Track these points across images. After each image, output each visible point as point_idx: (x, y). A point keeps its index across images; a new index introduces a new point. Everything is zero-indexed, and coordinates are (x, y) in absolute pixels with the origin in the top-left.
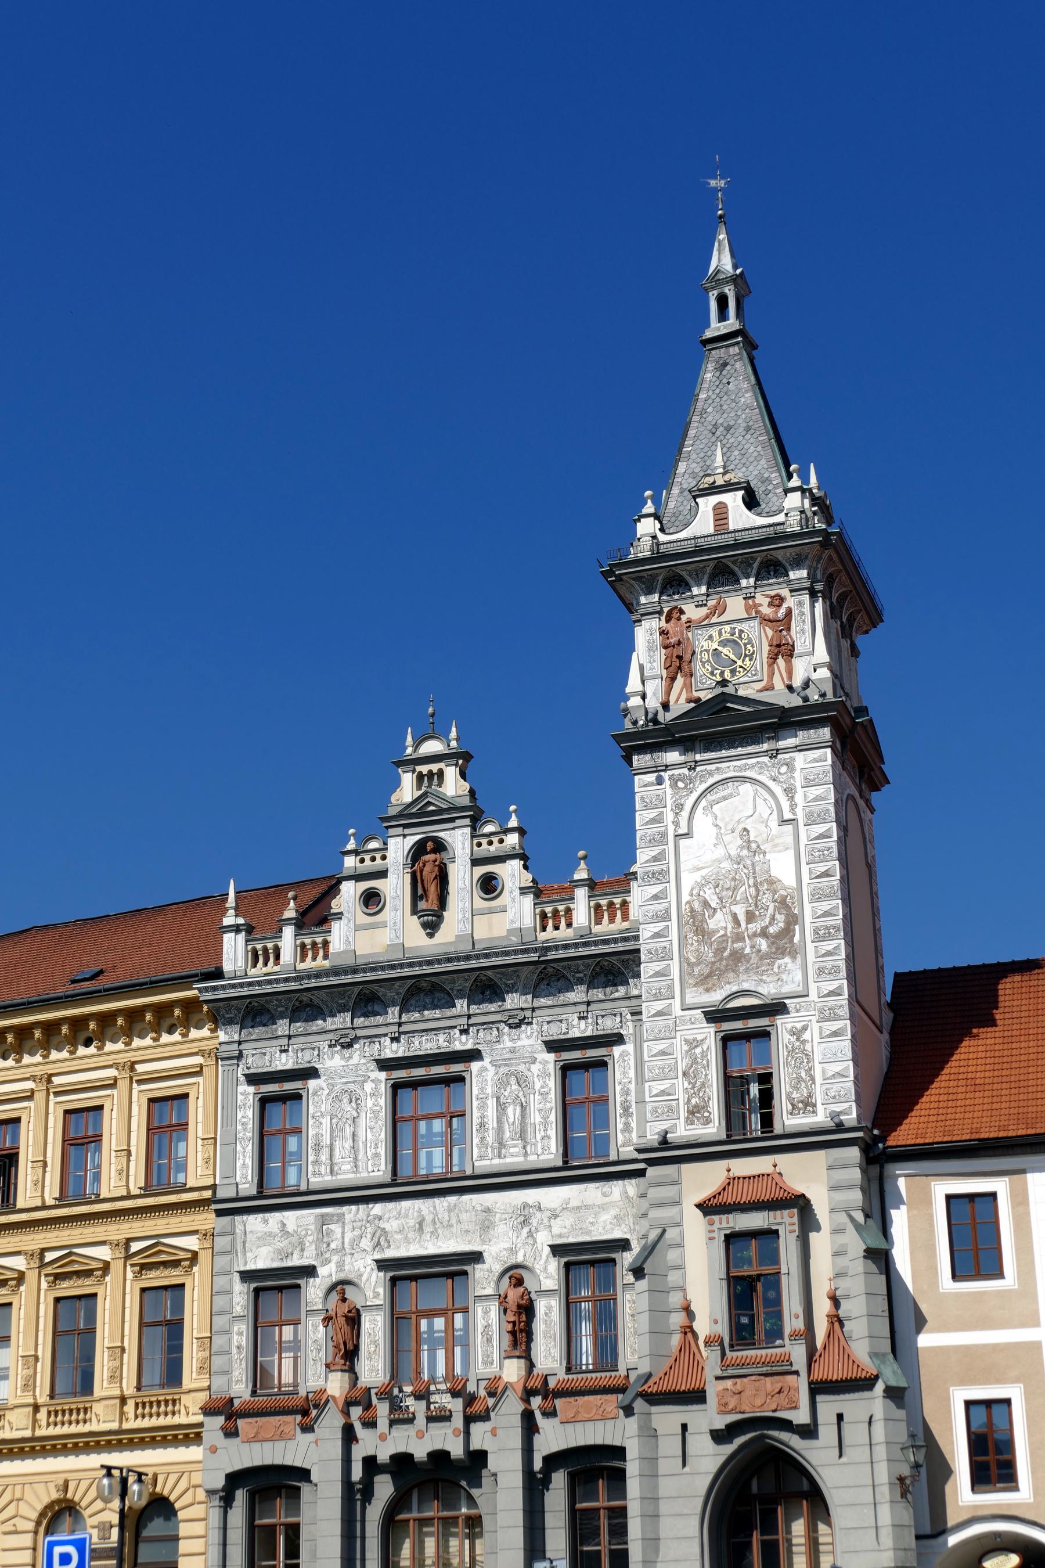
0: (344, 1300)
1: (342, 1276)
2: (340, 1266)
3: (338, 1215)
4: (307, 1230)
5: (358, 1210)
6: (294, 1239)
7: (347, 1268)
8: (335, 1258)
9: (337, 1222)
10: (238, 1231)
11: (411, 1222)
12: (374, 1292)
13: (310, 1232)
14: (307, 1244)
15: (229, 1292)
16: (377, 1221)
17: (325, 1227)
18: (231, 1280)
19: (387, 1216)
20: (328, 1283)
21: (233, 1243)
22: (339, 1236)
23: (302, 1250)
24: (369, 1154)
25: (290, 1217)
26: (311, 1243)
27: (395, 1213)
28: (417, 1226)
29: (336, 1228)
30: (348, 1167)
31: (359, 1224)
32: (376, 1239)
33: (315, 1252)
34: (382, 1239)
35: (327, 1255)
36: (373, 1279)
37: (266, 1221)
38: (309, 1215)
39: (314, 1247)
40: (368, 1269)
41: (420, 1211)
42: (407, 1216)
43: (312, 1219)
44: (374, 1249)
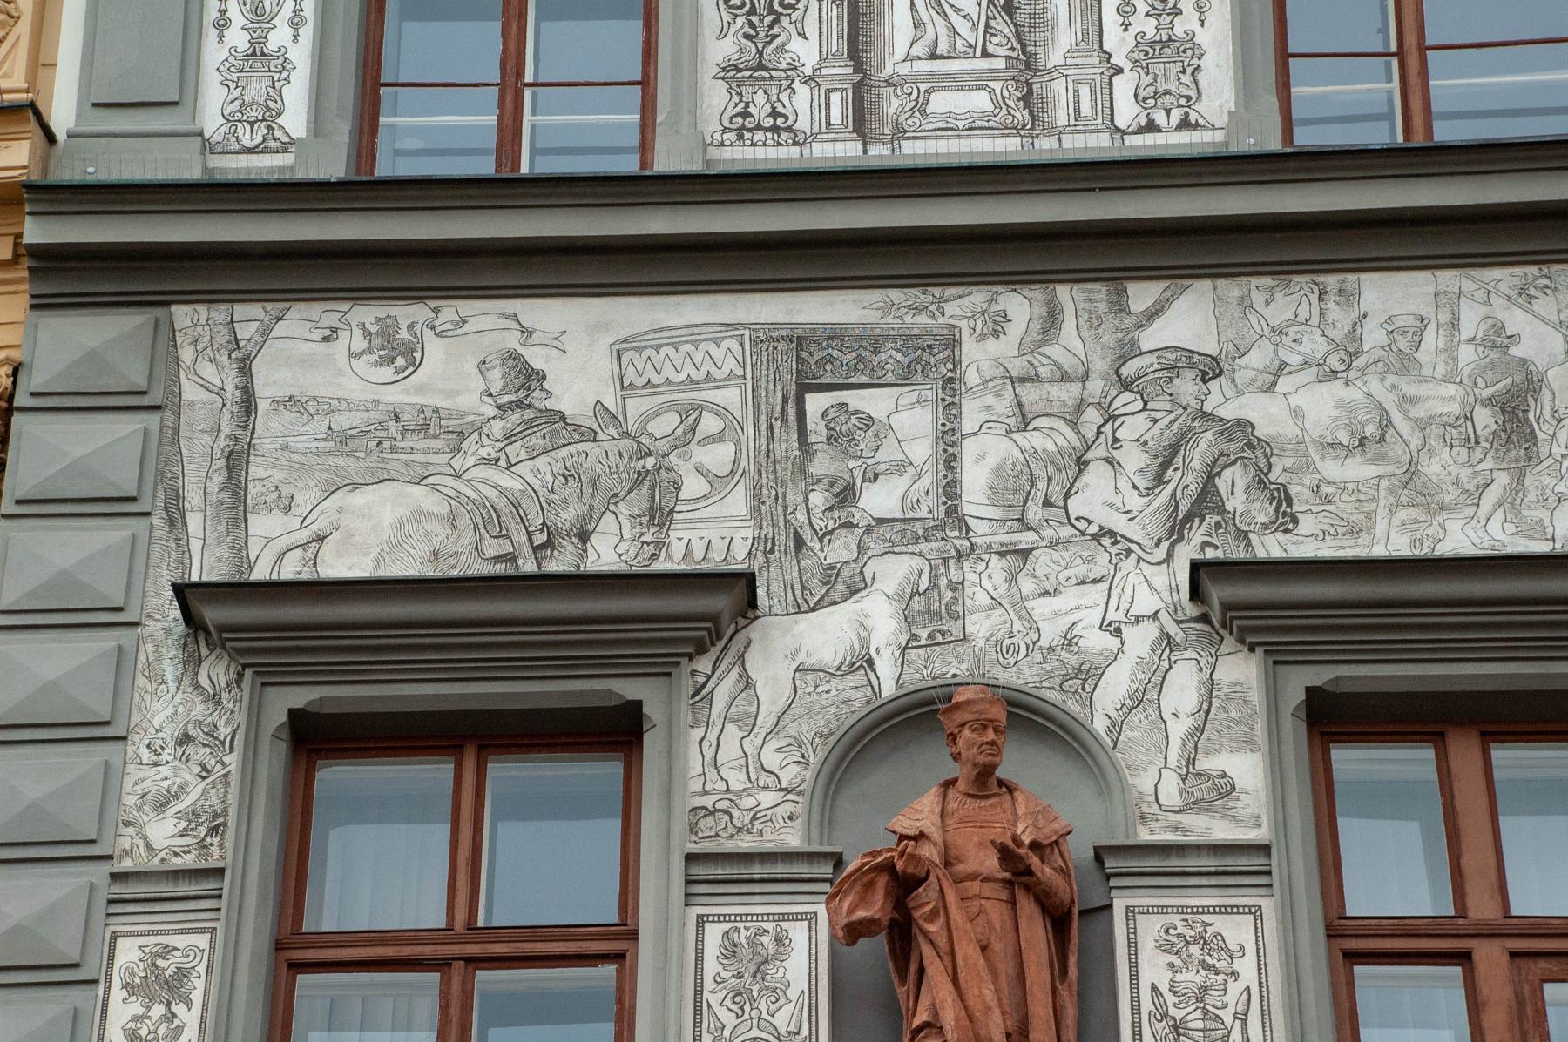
0: (986, 782)
1: (949, 666)
2: (932, 613)
3: (908, 339)
4: (691, 412)
5: (1053, 319)
6: (593, 456)
7: (980, 627)
8: (893, 572)
9: (905, 377)
10: (191, 392)
11: (1443, 400)
12: (1190, 770)
13: (710, 424)
14: (693, 486)
15: (98, 731)
16: (1187, 387)
17: (816, 404)
18: (121, 660)
19: (1258, 358)
20: (849, 700)
21: (162, 458)
22: (922, 451)
23: (660, 516)
24: (1117, 42)
25: (581, 345)
26: (718, 482)
27: (1315, 345)
28: (1485, 419)
29: (904, 416)
30: (980, 101)
31: (1065, 394)
32: (1185, 479)
33: (744, 534)
34: (1235, 486)
35: (840, 550)
36: (1182, 690)
37: (402, 354)
38: (708, 338)
39: (737, 502)
40: (1140, 640)
41: (1497, 338)
42: (1403, 362)
43: (727, 356)
44: (1176, 530)
